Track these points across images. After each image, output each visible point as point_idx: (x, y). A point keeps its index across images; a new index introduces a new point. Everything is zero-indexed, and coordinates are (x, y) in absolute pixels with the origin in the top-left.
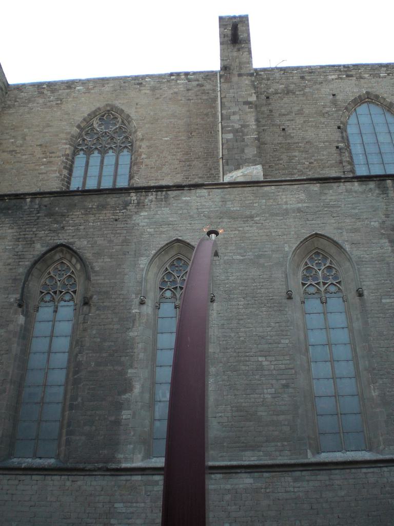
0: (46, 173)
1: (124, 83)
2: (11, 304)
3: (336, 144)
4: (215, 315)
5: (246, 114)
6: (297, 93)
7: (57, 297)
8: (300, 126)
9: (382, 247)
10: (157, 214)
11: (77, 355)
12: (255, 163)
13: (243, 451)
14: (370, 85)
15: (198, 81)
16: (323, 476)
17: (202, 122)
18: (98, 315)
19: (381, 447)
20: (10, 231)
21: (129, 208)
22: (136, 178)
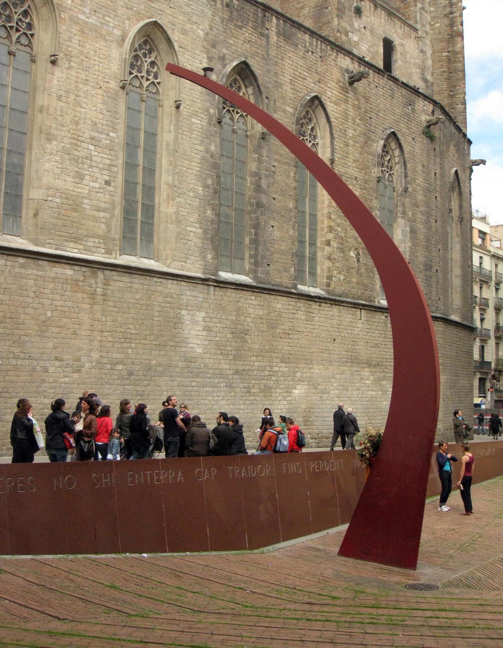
13: (67, 241)
16: (126, 278)
19: (169, 261)
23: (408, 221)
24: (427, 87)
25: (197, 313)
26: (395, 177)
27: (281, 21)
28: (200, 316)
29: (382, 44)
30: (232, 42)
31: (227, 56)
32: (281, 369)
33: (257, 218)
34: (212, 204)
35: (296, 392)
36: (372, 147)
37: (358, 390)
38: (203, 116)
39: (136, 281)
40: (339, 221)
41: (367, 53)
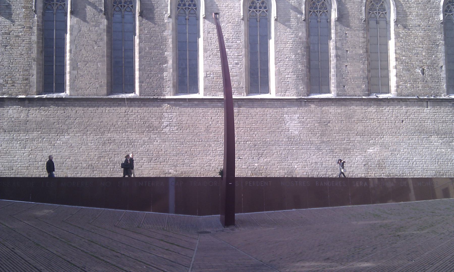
32: (357, 139)
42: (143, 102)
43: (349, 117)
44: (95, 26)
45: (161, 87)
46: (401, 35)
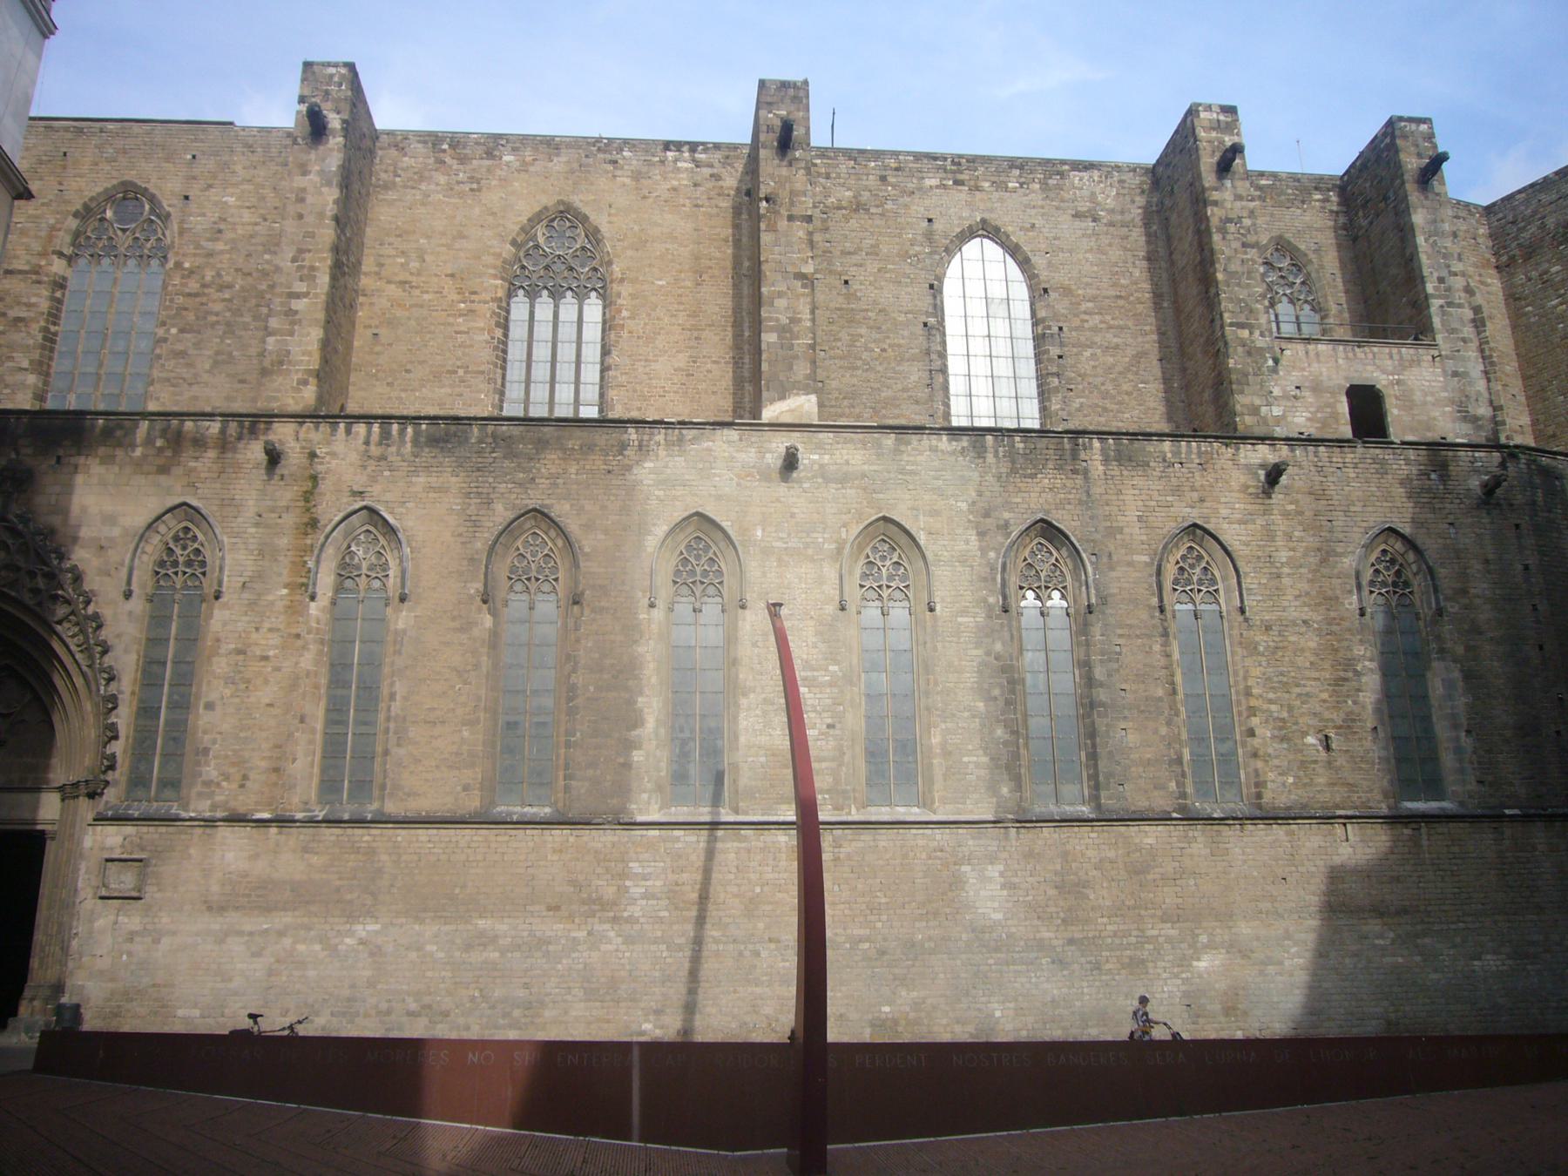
0: (467, 333)
1: (587, 156)
2: (471, 597)
3: (923, 319)
4: (748, 627)
5: (798, 297)
6: (873, 210)
7: (533, 586)
8: (872, 279)
9: (967, 542)
10: (666, 467)
11: (569, 676)
12: (807, 390)
14: (989, 205)
15: (711, 166)
16: (867, 836)
17: (718, 255)
18: (594, 620)
20: (454, 479)
21: (626, 453)
22: (614, 353)
23: (1455, 661)
24: (1479, 428)
25: (990, 867)
26: (1417, 599)
27: (1111, 441)
28: (994, 871)
29: (1344, 399)
30: (1019, 500)
31: (1012, 522)
32: (1163, 932)
33: (1093, 723)
34: (1005, 721)
35: (1202, 965)
36: (1339, 565)
37: (1356, 955)
38: (977, 610)
39: (884, 837)
40: (1271, 695)
41: (1309, 424)
42: (575, 832)
43: (1137, 871)
44: (461, 630)
45: (623, 790)
46: (1261, 649)
